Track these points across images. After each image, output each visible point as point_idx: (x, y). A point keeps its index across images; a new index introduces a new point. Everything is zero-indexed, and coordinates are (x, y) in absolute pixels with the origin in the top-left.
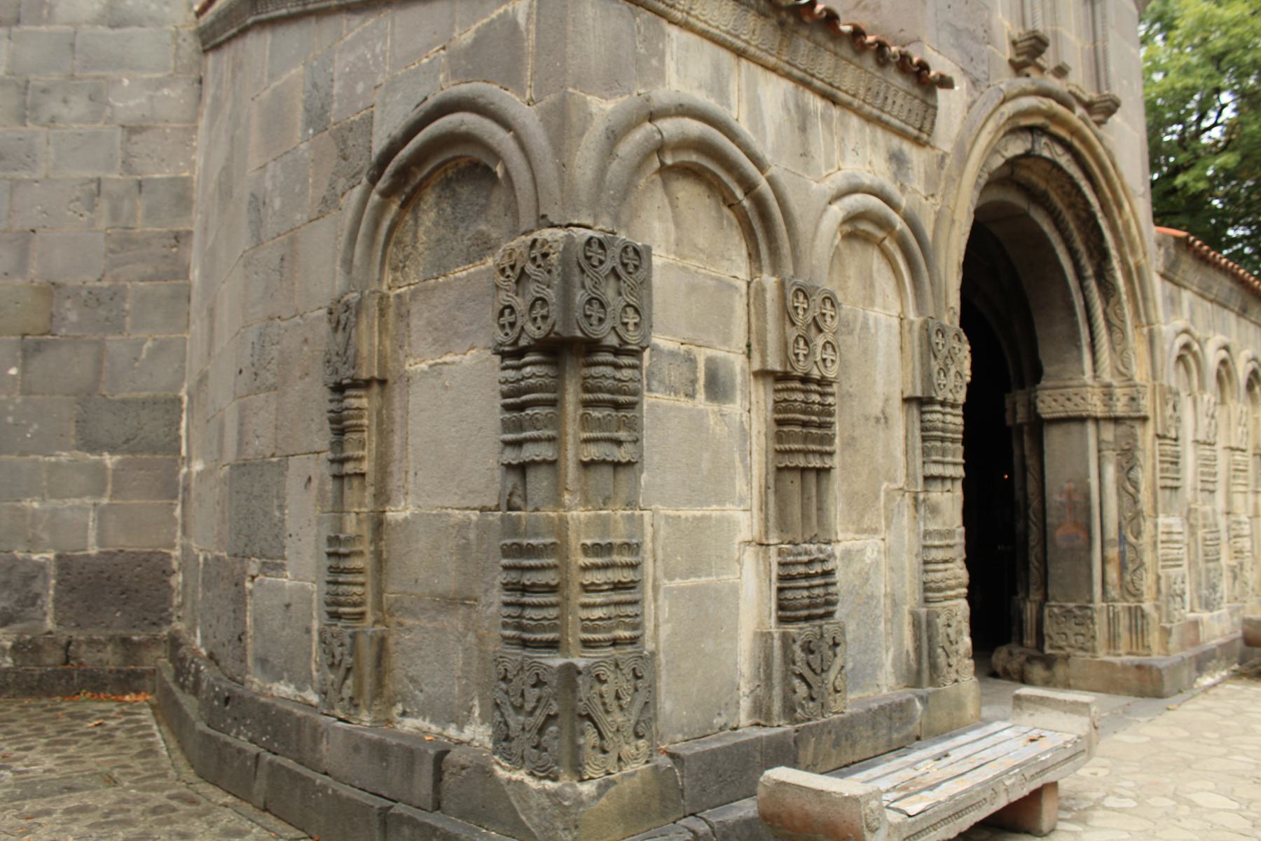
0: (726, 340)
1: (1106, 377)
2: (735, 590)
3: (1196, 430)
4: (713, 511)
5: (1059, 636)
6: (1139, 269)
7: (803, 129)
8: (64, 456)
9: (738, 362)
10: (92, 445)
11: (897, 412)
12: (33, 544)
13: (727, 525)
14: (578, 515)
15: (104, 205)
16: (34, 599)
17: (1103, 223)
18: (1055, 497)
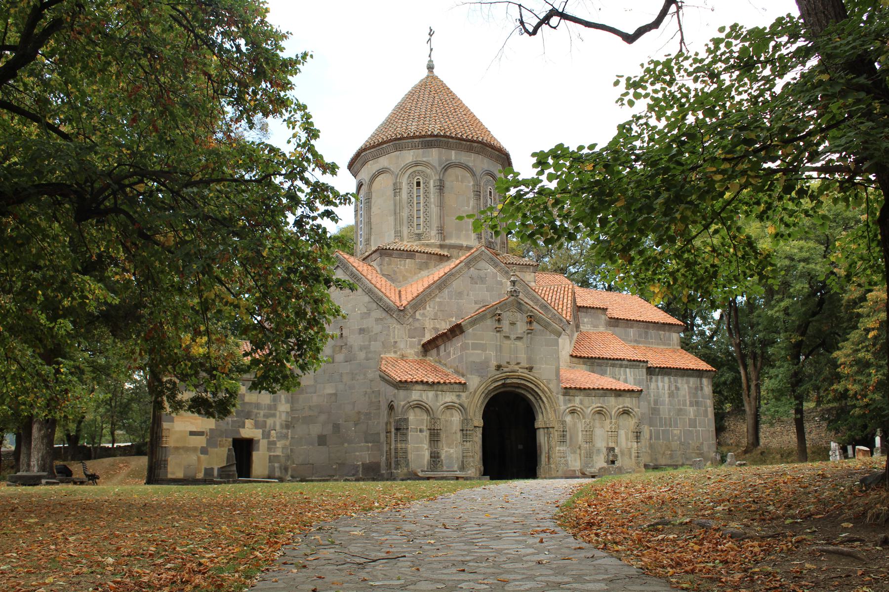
0: (423, 425)
1: (545, 419)
2: (424, 455)
5: (538, 473)
8: (362, 444)
10: (367, 442)
11: (458, 431)
12: (358, 461)
14: (399, 445)
15: (367, 396)
16: (358, 471)
17: (536, 390)
18: (538, 444)
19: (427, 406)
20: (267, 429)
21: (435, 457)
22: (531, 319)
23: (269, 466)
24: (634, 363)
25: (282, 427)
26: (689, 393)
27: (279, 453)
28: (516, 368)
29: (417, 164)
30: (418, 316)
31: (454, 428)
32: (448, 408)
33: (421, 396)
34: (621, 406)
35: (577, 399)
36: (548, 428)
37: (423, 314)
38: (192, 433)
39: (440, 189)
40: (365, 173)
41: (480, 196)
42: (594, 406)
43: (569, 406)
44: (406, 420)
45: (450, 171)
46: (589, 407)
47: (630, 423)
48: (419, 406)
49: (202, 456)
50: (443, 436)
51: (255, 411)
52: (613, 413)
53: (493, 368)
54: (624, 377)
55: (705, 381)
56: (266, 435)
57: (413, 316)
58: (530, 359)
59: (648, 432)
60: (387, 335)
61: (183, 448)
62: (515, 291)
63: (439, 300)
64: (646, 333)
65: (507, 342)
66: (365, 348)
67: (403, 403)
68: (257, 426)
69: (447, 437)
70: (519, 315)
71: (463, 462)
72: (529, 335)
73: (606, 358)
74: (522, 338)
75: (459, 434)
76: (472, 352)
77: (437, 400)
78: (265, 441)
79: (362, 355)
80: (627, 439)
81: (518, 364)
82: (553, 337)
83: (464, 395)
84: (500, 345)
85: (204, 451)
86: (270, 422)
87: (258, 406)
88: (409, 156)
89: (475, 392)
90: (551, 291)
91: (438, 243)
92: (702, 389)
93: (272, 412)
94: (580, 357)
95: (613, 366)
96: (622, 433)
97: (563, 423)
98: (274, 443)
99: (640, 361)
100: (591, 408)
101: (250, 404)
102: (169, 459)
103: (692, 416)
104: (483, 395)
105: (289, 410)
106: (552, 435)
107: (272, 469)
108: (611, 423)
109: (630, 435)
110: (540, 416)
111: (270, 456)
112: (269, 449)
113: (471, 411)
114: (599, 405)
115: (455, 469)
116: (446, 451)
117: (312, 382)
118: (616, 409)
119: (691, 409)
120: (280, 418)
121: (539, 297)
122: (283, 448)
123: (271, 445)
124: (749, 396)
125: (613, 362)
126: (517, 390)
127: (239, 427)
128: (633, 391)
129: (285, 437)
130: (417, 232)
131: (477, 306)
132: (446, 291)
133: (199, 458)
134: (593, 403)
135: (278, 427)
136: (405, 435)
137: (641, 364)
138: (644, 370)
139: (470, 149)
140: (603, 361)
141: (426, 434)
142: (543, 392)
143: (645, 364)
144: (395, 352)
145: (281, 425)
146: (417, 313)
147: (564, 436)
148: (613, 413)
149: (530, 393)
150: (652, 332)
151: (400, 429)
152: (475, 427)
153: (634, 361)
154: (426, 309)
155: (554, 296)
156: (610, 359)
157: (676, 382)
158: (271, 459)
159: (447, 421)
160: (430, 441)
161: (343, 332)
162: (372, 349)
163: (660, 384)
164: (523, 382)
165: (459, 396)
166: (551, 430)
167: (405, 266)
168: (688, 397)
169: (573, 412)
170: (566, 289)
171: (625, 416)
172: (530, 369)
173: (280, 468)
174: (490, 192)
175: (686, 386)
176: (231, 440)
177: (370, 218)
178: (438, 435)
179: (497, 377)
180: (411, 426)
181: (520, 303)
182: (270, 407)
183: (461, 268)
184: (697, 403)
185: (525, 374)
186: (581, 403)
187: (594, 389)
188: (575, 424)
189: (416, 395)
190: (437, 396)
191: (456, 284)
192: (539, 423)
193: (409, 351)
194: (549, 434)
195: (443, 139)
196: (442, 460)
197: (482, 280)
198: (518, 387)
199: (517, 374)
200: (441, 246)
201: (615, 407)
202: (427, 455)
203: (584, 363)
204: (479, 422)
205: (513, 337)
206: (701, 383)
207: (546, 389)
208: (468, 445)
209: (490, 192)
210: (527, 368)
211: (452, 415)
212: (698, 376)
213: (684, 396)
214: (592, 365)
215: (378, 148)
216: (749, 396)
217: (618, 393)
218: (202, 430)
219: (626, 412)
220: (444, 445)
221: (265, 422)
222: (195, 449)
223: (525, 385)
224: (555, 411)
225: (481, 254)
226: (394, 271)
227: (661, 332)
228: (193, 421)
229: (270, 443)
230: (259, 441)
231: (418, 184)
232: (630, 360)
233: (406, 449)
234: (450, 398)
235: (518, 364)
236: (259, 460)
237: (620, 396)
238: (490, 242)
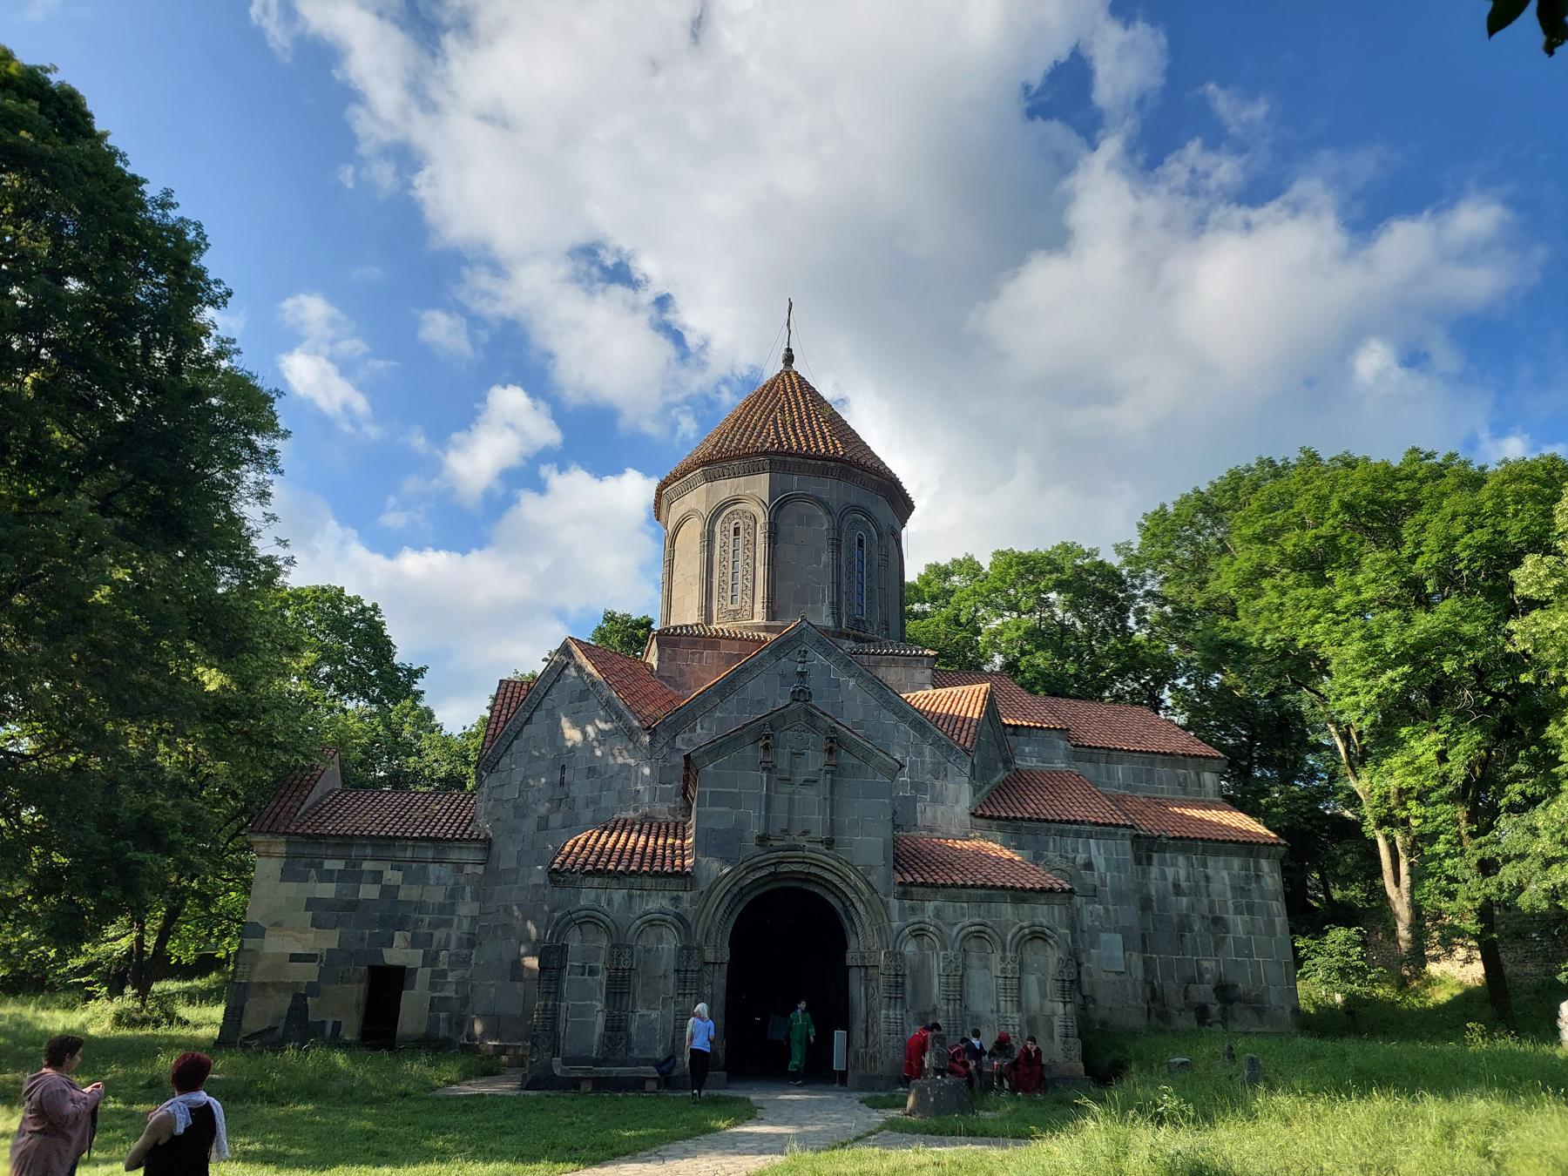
2: (594, 1023)
3: (939, 970)
4: (589, 1002)
6: (868, 901)
7: (630, 901)
9: (601, 966)
13: (596, 1006)
17: (843, 886)
19: (608, 920)
20: (434, 947)
21: (616, 1027)
22: (834, 744)
23: (429, 1018)
24: (1104, 830)
25: (460, 944)
26: (1233, 888)
27: (449, 992)
28: (802, 841)
29: (736, 501)
31: (663, 967)
32: (651, 923)
33: (598, 899)
34: (1025, 924)
35: (930, 907)
36: (867, 967)
37: (690, 740)
38: (295, 958)
39: (770, 537)
41: (839, 546)
42: (967, 921)
43: (911, 920)
44: (563, 950)
46: (956, 924)
47: (1050, 959)
48: (590, 920)
51: (416, 915)
52: (1009, 937)
53: (751, 845)
54: (1084, 856)
55: (1264, 864)
56: (430, 959)
58: (833, 827)
59: (1140, 964)
60: (626, 778)
61: (274, 984)
62: (801, 690)
63: (721, 715)
64: (1150, 773)
65: (787, 789)
66: (593, 802)
67: (557, 915)
68: (414, 944)
70: (811, 737)
71: (673, 1040)
72: (829, 776)
73: (1046, 820)
74: (815, 781)
75: (672, 979)
76: (710, 809)
77: (630, 908)
78: (428, 970)
80: (1043, 996)
81: (806, 833)
82: (880, 778)
83: (686, 896)
84: (768, 796)
86: (439, 935)
87: (420, 906)
88: (726, 488)
89: (710, 891)
90: (952, 698)
92: (1258, 877)
93: (449, 917)
94: (991, 817)
95: (1062, 834)
96: (1032, 980)
97: (896, 956)
98: (444, 974)
99: (1117, 825)
100: (959, 926)
101: (409, 902)
102: (247, 1004)
103: (1240, 932)
104: (729, 897)
105: (476, 914)
106: (874, 984)
107: (434, 1024)
108: (1003, 959)
109: (1051, 985)
110: (853, 943)
111: (433, 998)
112: (433, 986)
113: (699, 930)
114: (977, 920)
116: (642, 1016)
117: (513, 865)
118: (1015, 929)
119: (1239, 917)
120: (459, 928)
121: (908, 707)
122: (457, 983)
123: (438, 977)
124: (1397, 883)
125: (1061, 826)
126: (805, 886)
127: (383, 945)
128: (1052, 890)
129: (466, 962)
130: (731, 607)
132: (734, 698)
134: (964, 916)
135: (453, 945)
136: (558, 981)
137: (1121, 831)
138: (1128, 843)
139: (825, 473)
140: (1040, 825)
141: (602, 978)
142: (855, 889)
143: (1128, 832)
144: (636, 810)
145: (460, 939)
146: (678, 739)
147: (899, 986)
148: (1009, 937)
149: (832, 892)
150: (1162, 772)
151: (546, 968)
152: (707, 963)
153: (1104, 824)
154: (693, 730)
155: (954, 705)
156: (1053, 821)
157: (1205, 866)
158: (435, 1005)
159: (649, 951)
160: (607, 993)
161: (566, 776)
162: (603, 804)
163: (1170, 872)
164: (813, 870)
165: (676, 900)
166: (870, 971)
167: (700, 661)
168: (1229, 895)
169: (919, 934)
170: (976, 693)
171: (1039, 942)
172: (830, 843)
173: (450, 1022)
174: (861, 542)
175: (1225, 874)
176: (364, 969)
179: (757, 859)
180: (573, 962)
181: (812, 715)
182: (442, 908)
183: (762, 658)
184: (1250, 909)
185: (821, 855)
186: (938, 913)
187: (964, 886)
188: (924, 960)
189: (588, 896)
190: (630, 897)
192: (851, 958)
193: (658, 807)
194: (867, 978)
195: (777, 458)
196: (629, 1036)
198: (807, 881)
199: (800, 853)
200: (767, 629)
201: (1014, 924)
202: (600, 1021)
203: (1000, 829)
204: (718, 951)
205: (800, 779)
206: (1258, 868)
207: (861, 885)
209: (861, 542)
210: (822, 842)
211: (660, 939)
212: (1249, 855)
213: (1223, 893)
214: (1017, 830)
215: (682, 480)
216: (1397, 883)
217: (1021, 895)
218: (314, 952)
219: (1038, 935)
220: (638, 1003)
221: (432, 934)
223: (820, 877)
224: (879, 931)
225: (800, 634)
226: (682, 673)
227: (1180, 771)
228: (298, 935)
229: (435, 974)
230: (416, 969)
231: (736, 532)
232: (1097, 824)
234: (657, 902)
235: (806, 833)
237: (1024, 901)
238: (858, 622)
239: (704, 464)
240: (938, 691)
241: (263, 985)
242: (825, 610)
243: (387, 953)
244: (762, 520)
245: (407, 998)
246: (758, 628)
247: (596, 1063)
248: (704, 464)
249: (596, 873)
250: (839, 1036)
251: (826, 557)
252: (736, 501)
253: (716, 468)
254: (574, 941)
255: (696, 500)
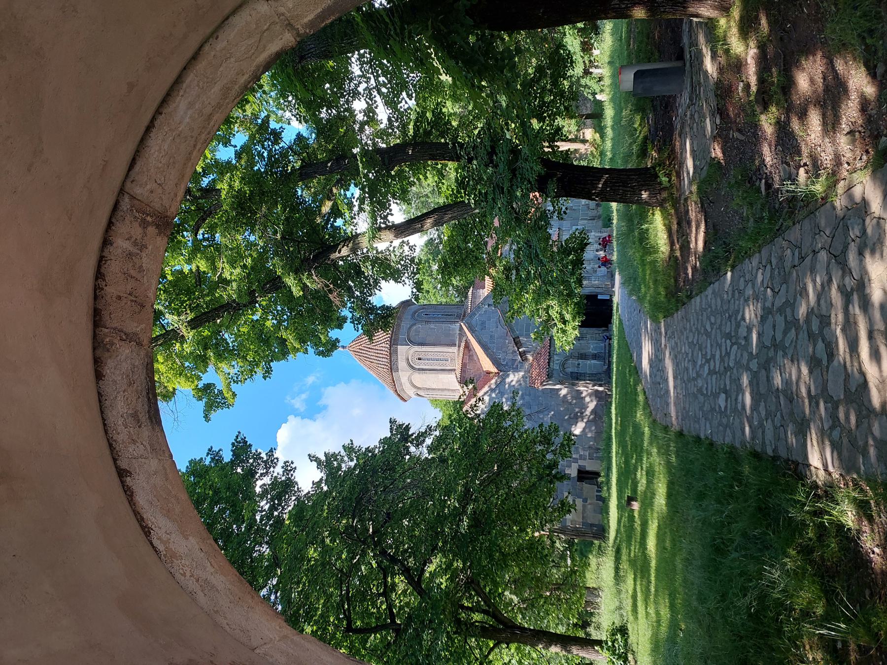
21: (595, 357)
30: (505, 363)
40: (410, 392)
45: (412, 340)
48: (563, 365)
49: (589, 501)
50: (582, 351)
57: (505, 366)
61: (583, 514)
67: (561, 375)
68: (570, 466)
69: (583, 349)
75: (581, 342)
79: (527, 398)
85: (585, 500)
88: (402, 364)
91: (457, 348)
112: (585, 459)
115: (603, 345)
123: (582, 457)
131: (499, 326)
133: (590, 504)
136: (581, 373)
154: (500, 359)
177: (439, 390)
178: (581, 354)
189: (556, 367)
191: (485, 339)
197: (483, 323)
200: (459, 347)
202: (593, 362)
208: (588, 336)
222: (584, 506)
231: (420, 359)
233: (589, 374)
236: (590, 466)
239: (391, 372)
240: (486, 286)
241: (583, 518)
242: (453, 326)
243: (572, 476)
244: (417, 348)
245: (588, 469)
246: (459, 350)
247: (605, 362)
248: (391, 372)
249: (549, 363)
250: (600, 297)
251: (432, 326)
252: (408, 359)
253: (394, 367)
254: (569, 370)
255: (404, 375)
